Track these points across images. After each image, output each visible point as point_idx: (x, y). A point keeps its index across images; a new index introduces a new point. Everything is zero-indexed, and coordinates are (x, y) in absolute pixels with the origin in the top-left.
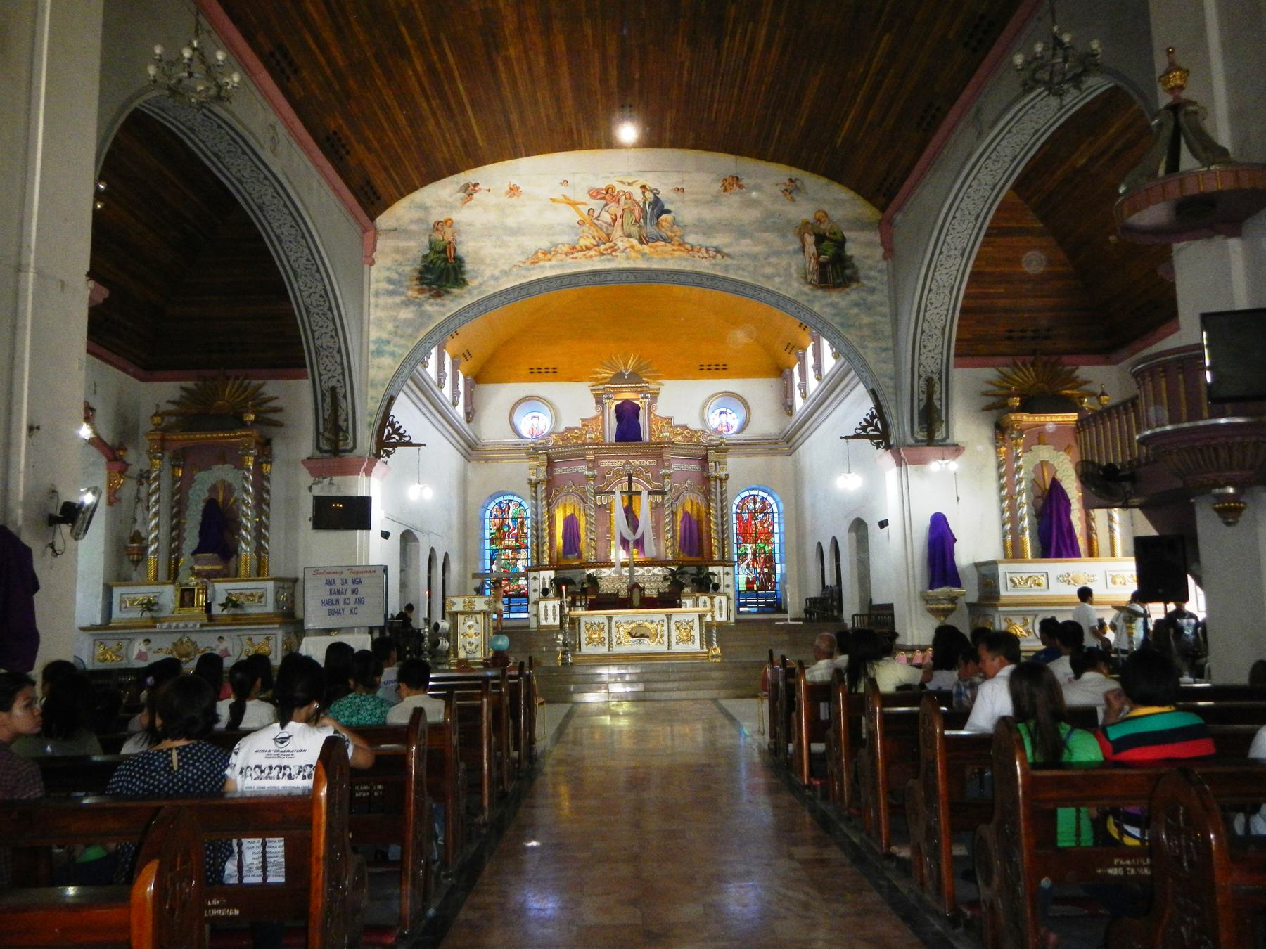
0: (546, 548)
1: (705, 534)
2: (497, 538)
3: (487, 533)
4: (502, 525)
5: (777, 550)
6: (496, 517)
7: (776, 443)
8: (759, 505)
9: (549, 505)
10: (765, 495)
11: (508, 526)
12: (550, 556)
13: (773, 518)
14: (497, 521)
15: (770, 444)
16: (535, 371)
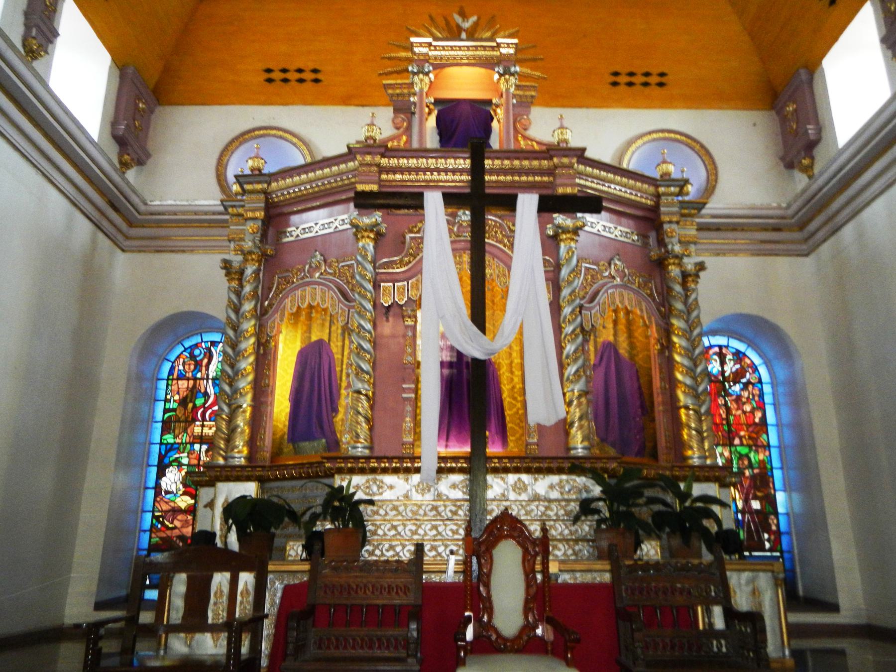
0: (241, 422)
1: (658, 399)
2: (178, 420)
3: (160, 407)
4: (193, 392)
5: (776, 463)
6: (181, 377)
7: (777, 229)
8: (730, 367)
9: (261, 315)
10: (741, 347)
11: (206, 395)
12: (252, 443)
13: (761, 395)
14: (183, 384)
15: (764, 228)
16: (277, 75)
